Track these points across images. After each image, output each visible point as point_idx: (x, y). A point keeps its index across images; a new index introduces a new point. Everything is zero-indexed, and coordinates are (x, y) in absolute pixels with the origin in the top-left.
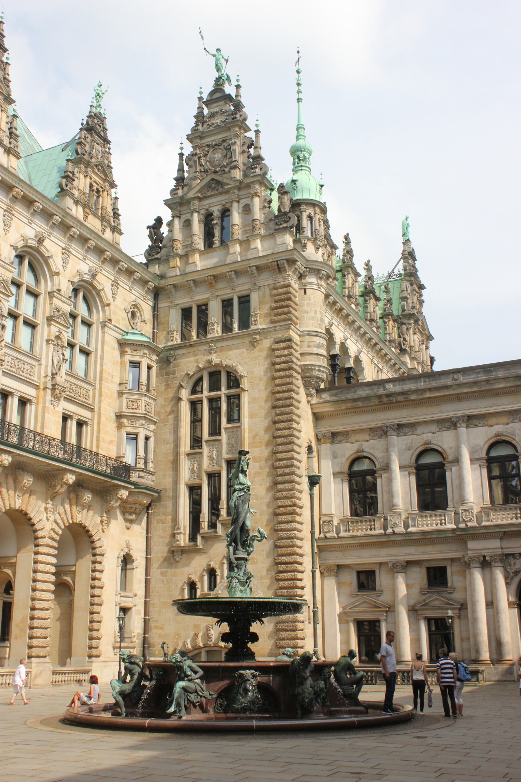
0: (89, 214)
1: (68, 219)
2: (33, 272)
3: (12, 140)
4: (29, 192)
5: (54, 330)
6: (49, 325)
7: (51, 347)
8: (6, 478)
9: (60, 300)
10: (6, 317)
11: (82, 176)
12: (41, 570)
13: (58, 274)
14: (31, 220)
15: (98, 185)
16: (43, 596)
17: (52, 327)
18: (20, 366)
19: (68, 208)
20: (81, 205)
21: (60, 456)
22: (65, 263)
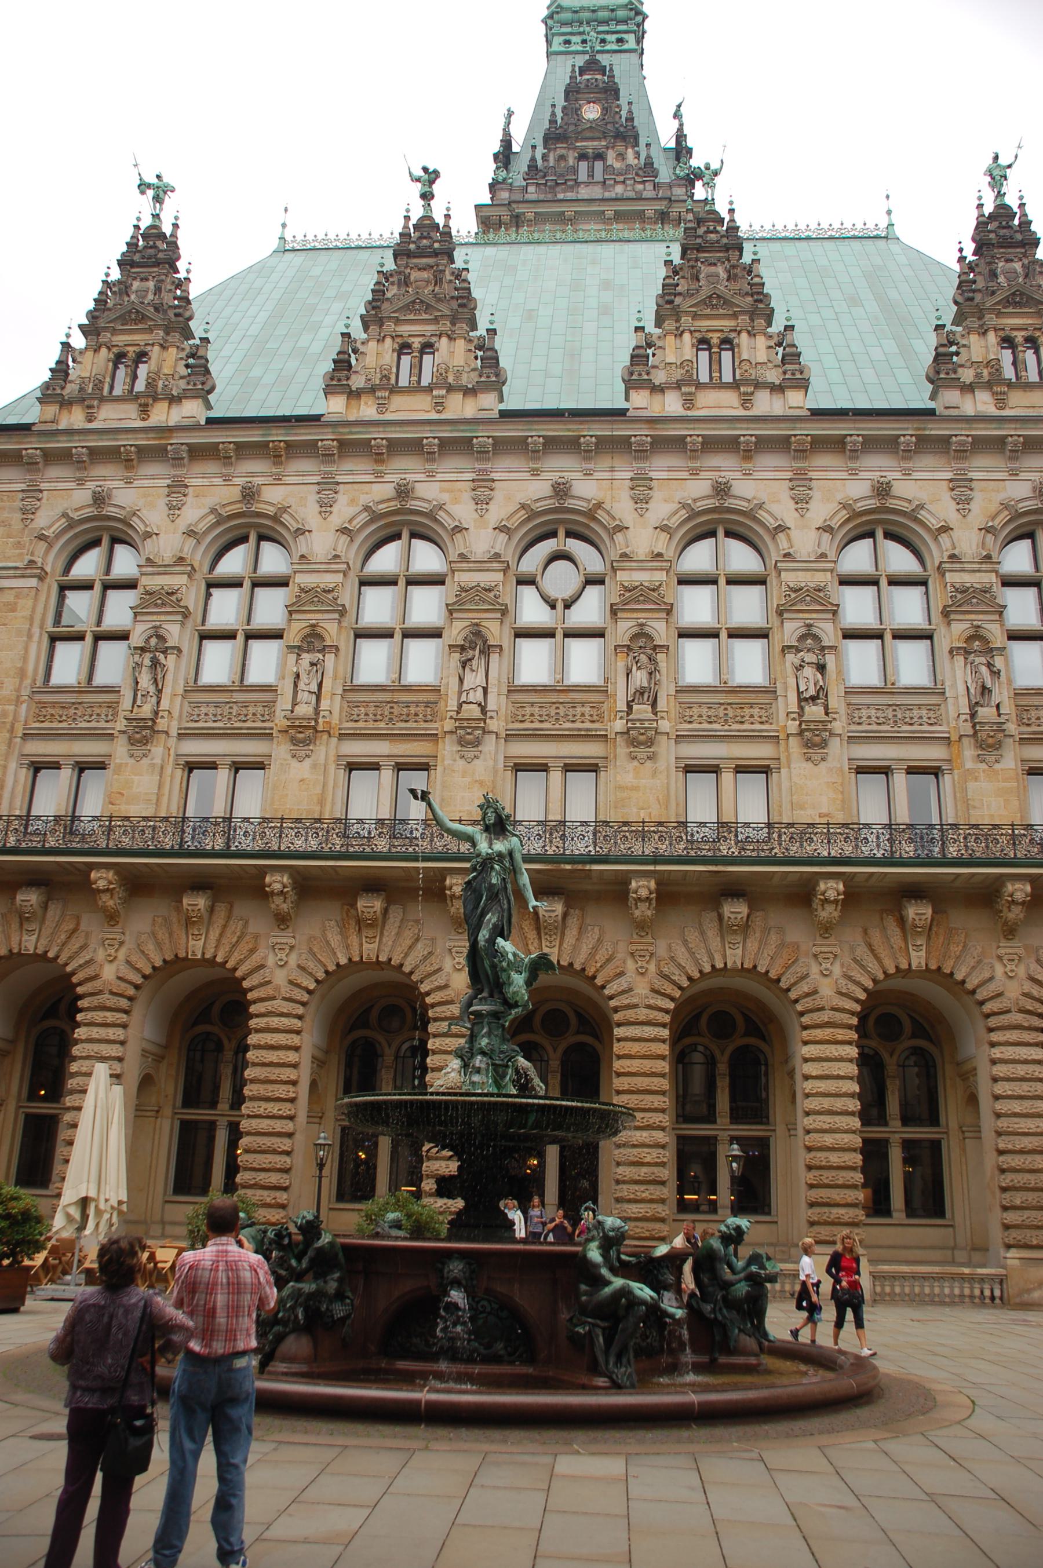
0: (1004, 393)
1: (931, 429)
2: (907, 547)
3: (788, 367)
4: (824, 429)
5: (960, 628)
6: (949, 624)
7: (960, 660)
8: (882, 919)
9: (963, 571)
10: (834, 648)
11: (974, 338)
12: (1002, 1075)
13: (945, 529)
14: (852, 470)
15: (1026, 329)
16: (1016, 1126)
17: (954, 625)
18: (900, 716)
19: (946, 408)
20: (979, 387)
21: (978, 854)
22: (963, 503)
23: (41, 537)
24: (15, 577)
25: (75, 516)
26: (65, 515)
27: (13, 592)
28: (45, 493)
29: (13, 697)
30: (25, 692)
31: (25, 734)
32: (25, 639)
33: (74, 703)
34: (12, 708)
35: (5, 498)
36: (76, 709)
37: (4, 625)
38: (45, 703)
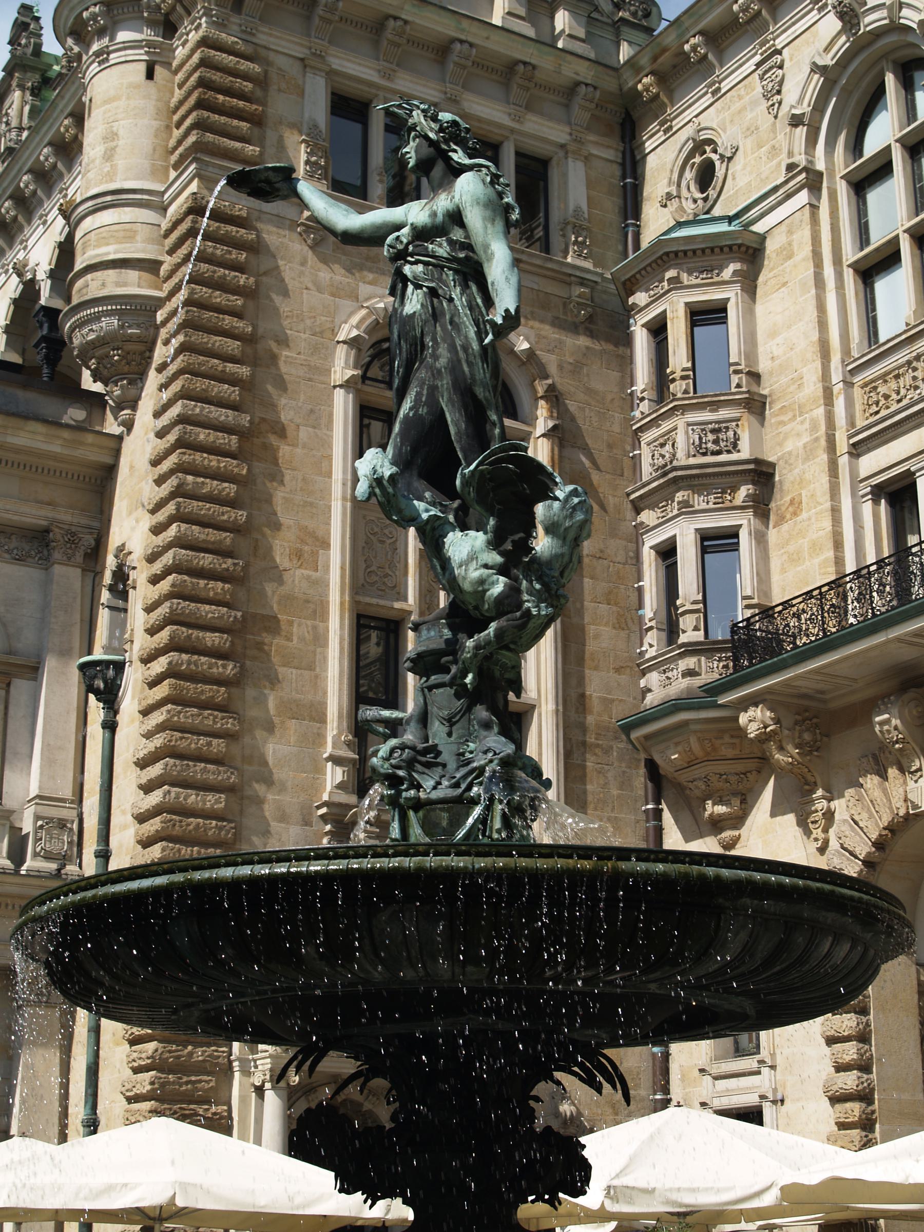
23: (796, 121)
24: (780, 203)
25: (828, 60)
26: (816, 68)
27: (783, 227)
28: (785, 51)
29: (820, 392)
30: (836, 376)
31: (854, 445)
32: (813, 291)
33: (909, 363)
34: (820, 411)
35: (742, 92)
36: (915, 369)
37: (785, 284)
38: (873, 381)
